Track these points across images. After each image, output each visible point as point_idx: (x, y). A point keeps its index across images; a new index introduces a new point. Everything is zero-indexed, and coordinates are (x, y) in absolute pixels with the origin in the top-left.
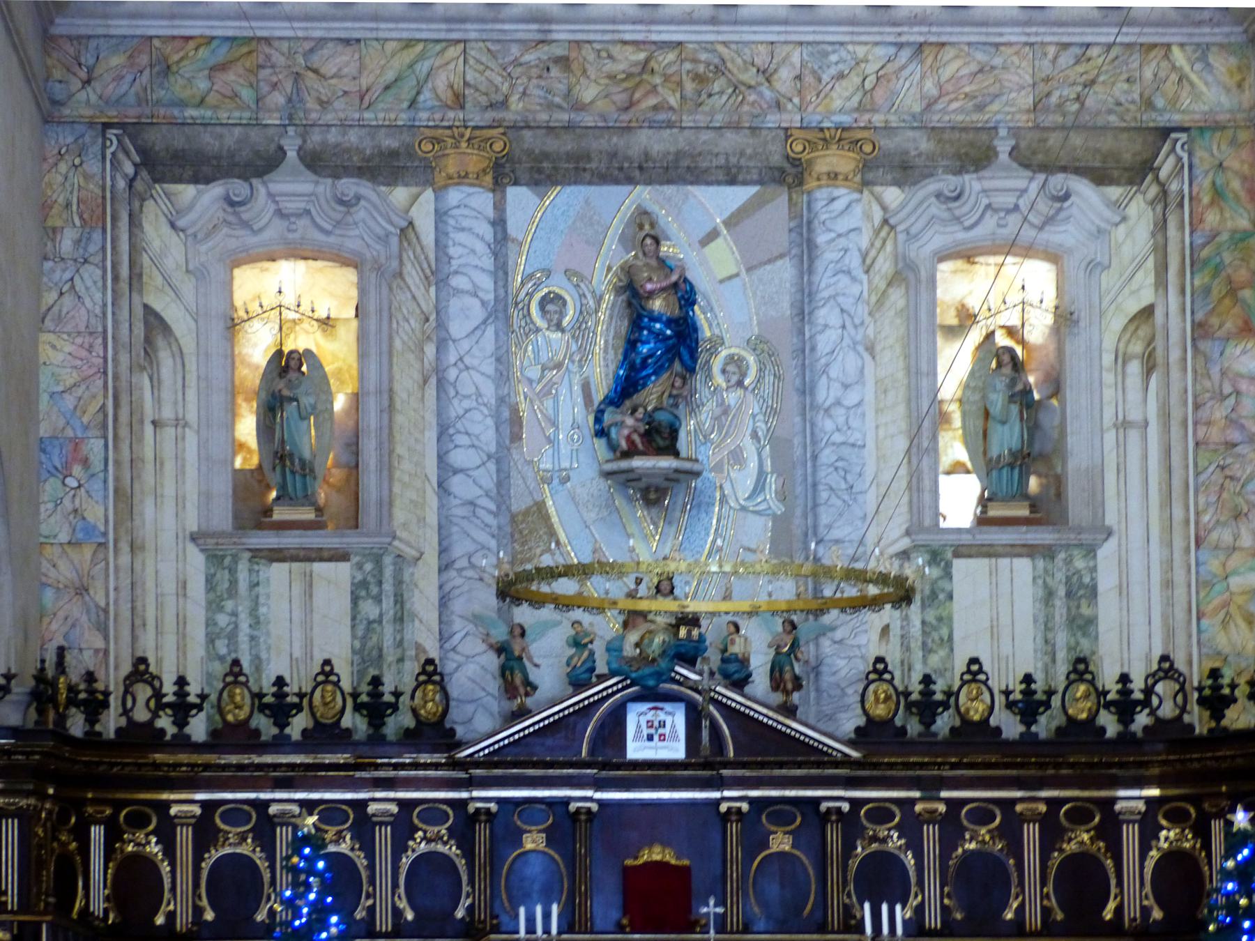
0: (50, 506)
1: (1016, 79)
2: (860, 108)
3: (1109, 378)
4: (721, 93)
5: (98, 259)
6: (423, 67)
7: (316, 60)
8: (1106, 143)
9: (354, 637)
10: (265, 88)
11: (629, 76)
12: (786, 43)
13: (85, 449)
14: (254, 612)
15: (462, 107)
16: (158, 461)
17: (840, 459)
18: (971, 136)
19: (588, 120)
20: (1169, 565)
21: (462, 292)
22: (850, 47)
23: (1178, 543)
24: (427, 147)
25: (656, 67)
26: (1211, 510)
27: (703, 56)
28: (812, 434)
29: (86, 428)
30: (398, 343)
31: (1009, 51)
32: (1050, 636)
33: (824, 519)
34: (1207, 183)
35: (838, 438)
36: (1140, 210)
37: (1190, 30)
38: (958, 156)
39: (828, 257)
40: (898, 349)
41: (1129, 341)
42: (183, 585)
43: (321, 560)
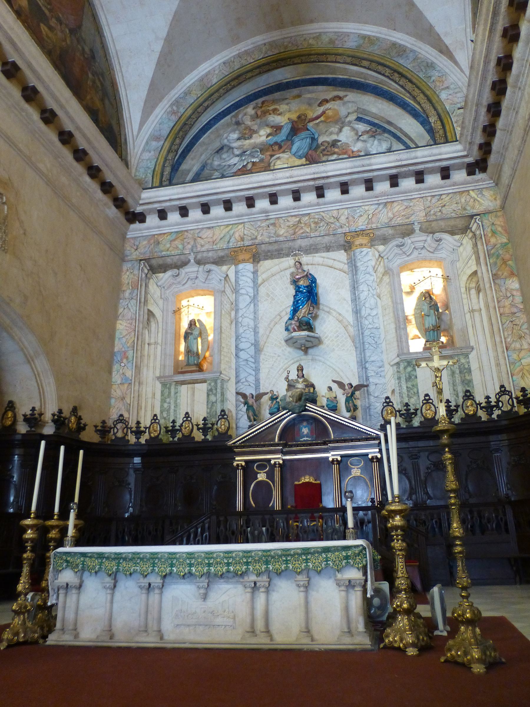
0: (116, 372)
1: (418, 208)
2: (368, 224)
3: (464, 296)
4: (323, 226)
5: (135, 298)
6: (232, 232)
7: (200, 235)
8: (452, 223)
9: (207, 408)
10: (186, 244)
11: (294, 225)
13: (127, 354)
14: (176, 401)
15: (243, 241)
16: (149, 356)
17: (372, 333)
18: (406, 227)
19: (281, 239)
20: (497, 358)
21: (244, 294)
22: (363, 207)
23: (500, 350)
24: (232, 253)
25: (302, 221)
26: (510, 337)
27: (317, 217)
28: (361, 326)
29: (128, 347)
30: (223, 312)
31: (415, 201)
32: (455, 388)
33: (368, 354)
34: (489, 230)
35: (370, 326)
36: (467, 242)
38: (402, 234)
39: (361, 268)
40: (388, 296)
41: (470, 283)
42: (154, 394)
43: (198, 383)
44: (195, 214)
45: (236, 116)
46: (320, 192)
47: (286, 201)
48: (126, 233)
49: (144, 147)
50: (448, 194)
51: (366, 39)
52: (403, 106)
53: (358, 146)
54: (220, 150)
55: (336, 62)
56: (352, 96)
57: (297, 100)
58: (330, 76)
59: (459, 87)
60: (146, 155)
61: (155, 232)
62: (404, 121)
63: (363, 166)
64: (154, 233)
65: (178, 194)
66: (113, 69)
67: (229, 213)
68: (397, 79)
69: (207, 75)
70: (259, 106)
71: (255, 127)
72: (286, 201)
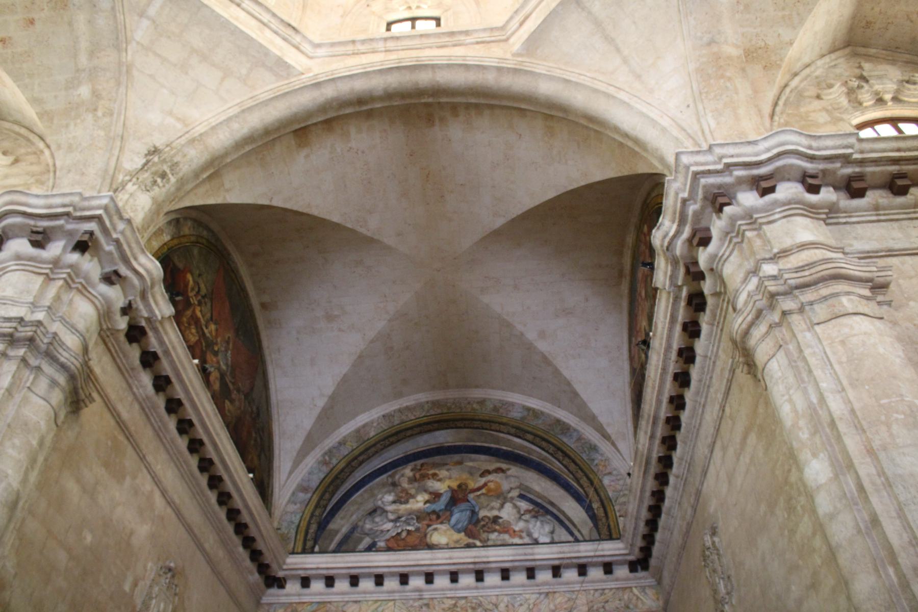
1: (581, 602)
12: (502, 595)
22: (524, 595)
27: (475, 601)
37: (638, 581)
44: (342, 585)
45: (392, 476)
46: (479, 576)
47: (442, 582)
48: (261, 598)
49: (290, 498)
50: (611, 589)
51: (531, 412)
52: (566, 487)
53: (520, 526)
54: (373, 512)
55: (500, 431)
56: (515, 470)
57: (459, 467)
58: (493, 445)
59: (621, 475)
60: (291, 508)
61: (295, 599)
62: (567, 504)
63: (525, 554)
64: (293, 601)
65: (327, 563)
66: (272, 420)
67: (379, 588)
68: (561, 458)
69: (364, 426)
70: (419, 467)
71: (413, 492)
72: (442, 582)
